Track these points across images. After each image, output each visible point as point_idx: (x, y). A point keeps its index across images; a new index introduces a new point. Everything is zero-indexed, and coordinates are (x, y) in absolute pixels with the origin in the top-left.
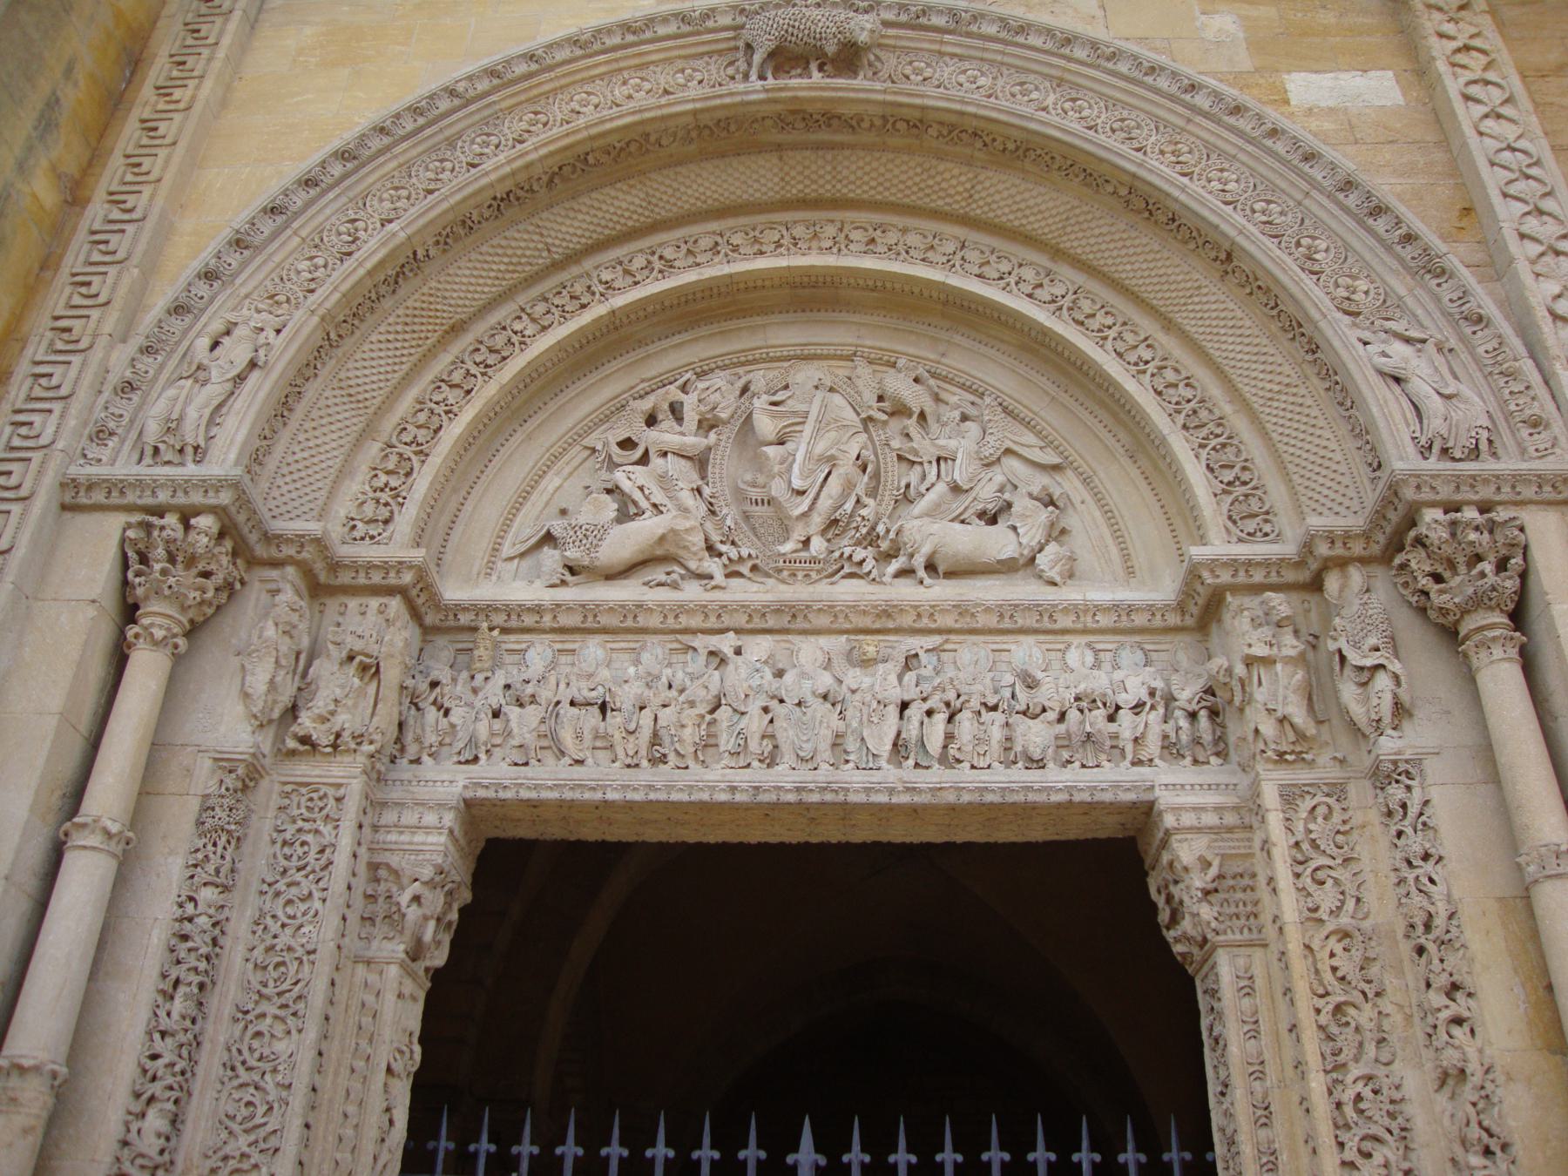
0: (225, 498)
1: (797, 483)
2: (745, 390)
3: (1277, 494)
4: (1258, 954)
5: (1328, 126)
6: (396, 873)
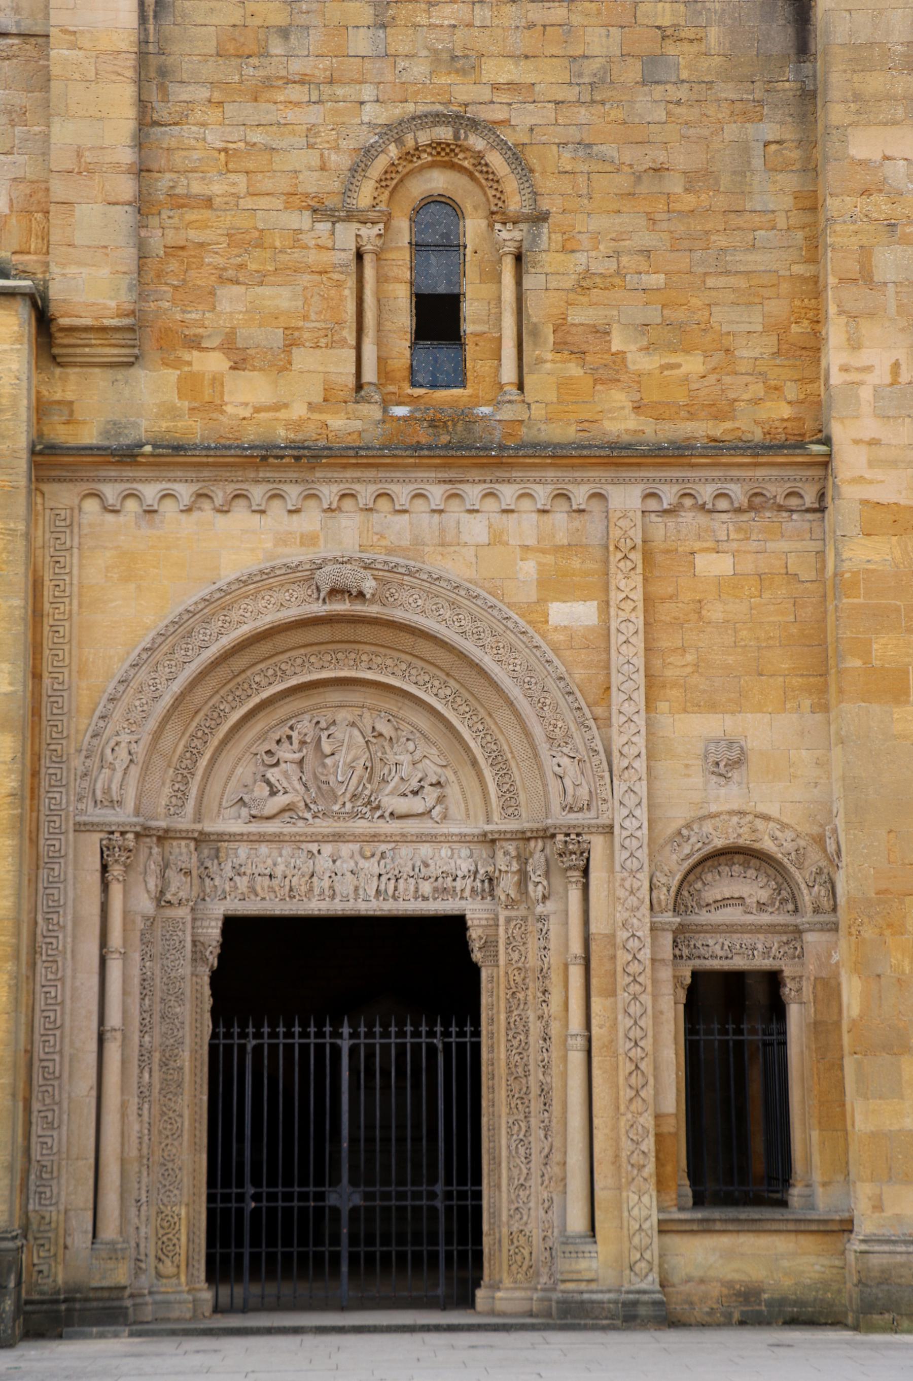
0: (138, 829)
1: (340, 779)
2: (318, 722)
3: (522, 798)
4: (495, 969)
5: (562, 638)
6: (203, 944)
